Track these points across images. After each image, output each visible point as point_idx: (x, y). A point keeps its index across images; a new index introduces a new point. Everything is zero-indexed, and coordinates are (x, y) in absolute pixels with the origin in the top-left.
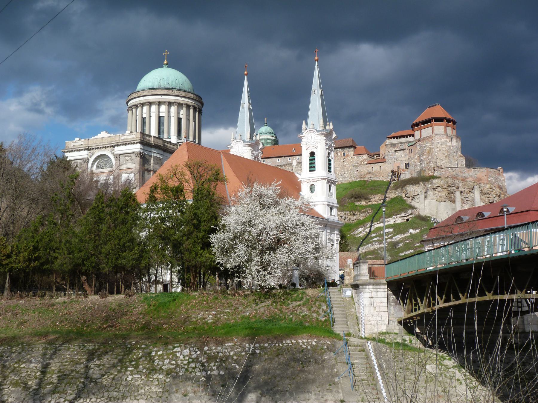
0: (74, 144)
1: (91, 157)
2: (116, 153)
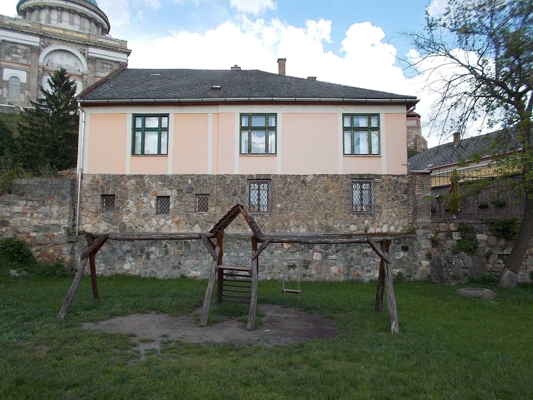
2: (89, 54)
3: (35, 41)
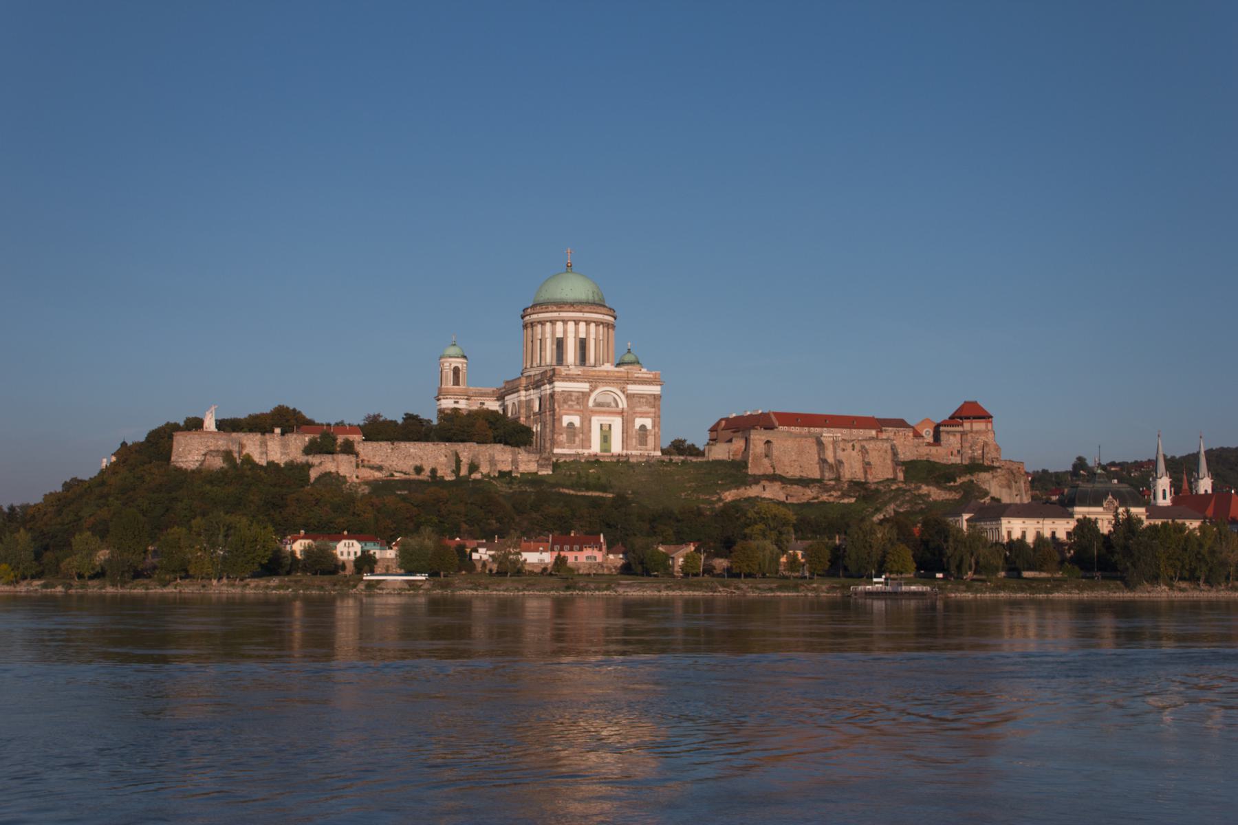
0: (566, 372)
1: (591, 391)
2: (629, 392)
3: (585, 387)
